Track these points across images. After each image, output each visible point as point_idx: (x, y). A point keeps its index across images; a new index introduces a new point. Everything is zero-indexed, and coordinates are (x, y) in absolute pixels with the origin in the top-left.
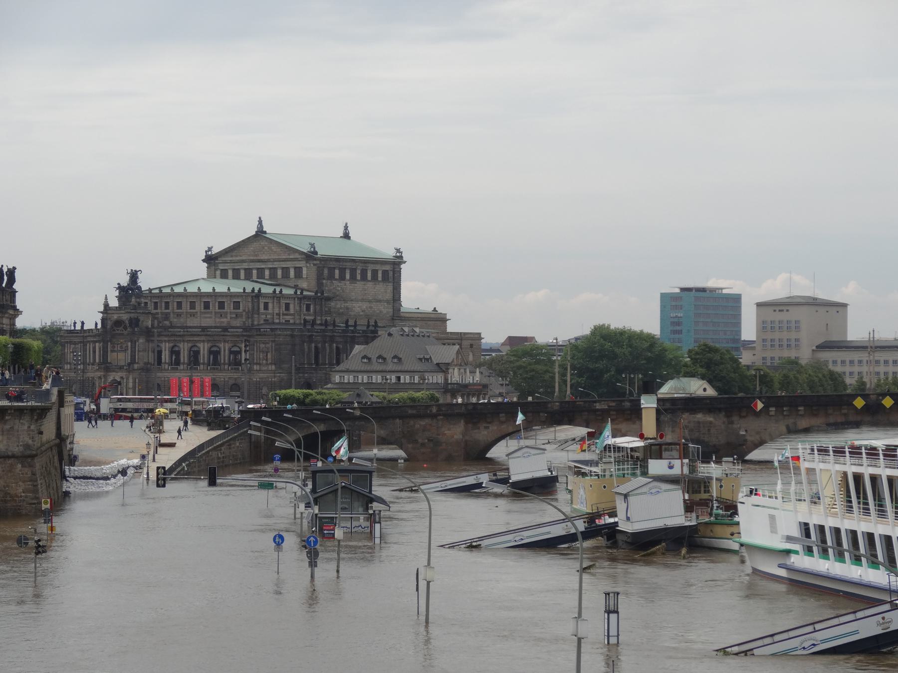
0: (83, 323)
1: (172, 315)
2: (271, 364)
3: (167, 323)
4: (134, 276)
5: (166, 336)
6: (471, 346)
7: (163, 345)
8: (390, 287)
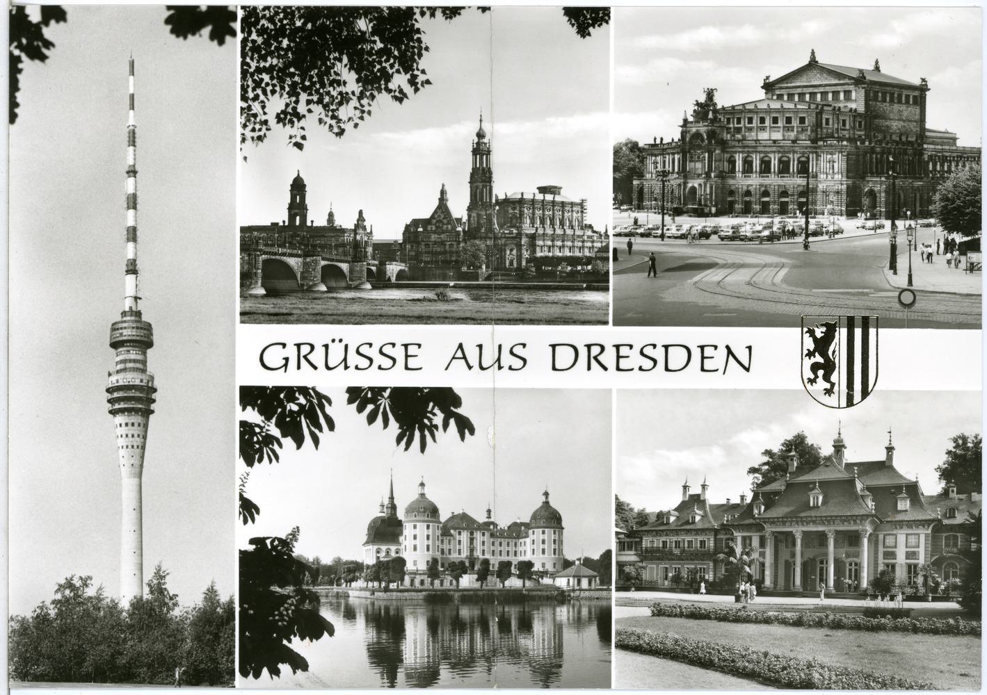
0: (662, 139)
3: (739, 136)
4: (710, 94)
5: (740, 147)
7: (737, 156)
8: (918, 111)
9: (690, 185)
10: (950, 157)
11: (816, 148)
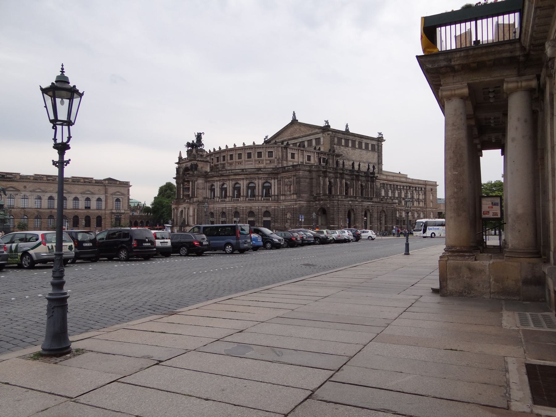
1: (226, 165)
2: (293, 194)
4: (199, 137)
6: (432, 189)
7: (215, 184)
9: (180, 210)
10: (400, 186)
11: (278, 174)
